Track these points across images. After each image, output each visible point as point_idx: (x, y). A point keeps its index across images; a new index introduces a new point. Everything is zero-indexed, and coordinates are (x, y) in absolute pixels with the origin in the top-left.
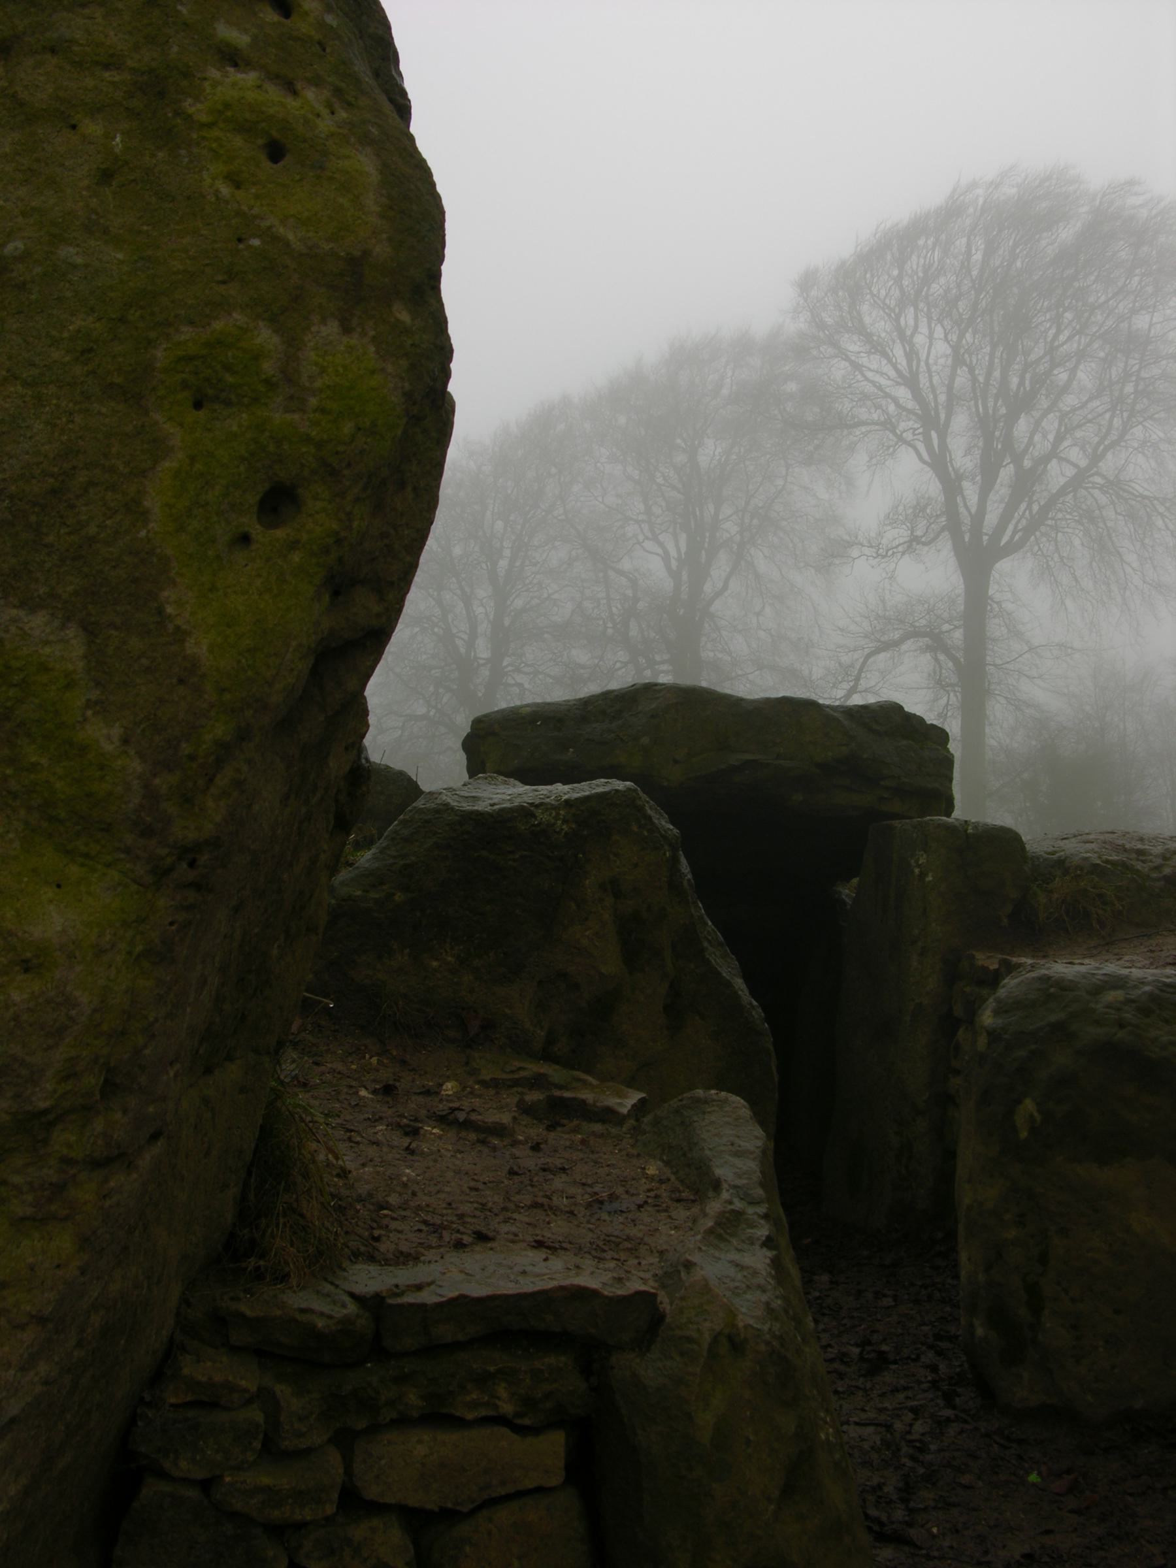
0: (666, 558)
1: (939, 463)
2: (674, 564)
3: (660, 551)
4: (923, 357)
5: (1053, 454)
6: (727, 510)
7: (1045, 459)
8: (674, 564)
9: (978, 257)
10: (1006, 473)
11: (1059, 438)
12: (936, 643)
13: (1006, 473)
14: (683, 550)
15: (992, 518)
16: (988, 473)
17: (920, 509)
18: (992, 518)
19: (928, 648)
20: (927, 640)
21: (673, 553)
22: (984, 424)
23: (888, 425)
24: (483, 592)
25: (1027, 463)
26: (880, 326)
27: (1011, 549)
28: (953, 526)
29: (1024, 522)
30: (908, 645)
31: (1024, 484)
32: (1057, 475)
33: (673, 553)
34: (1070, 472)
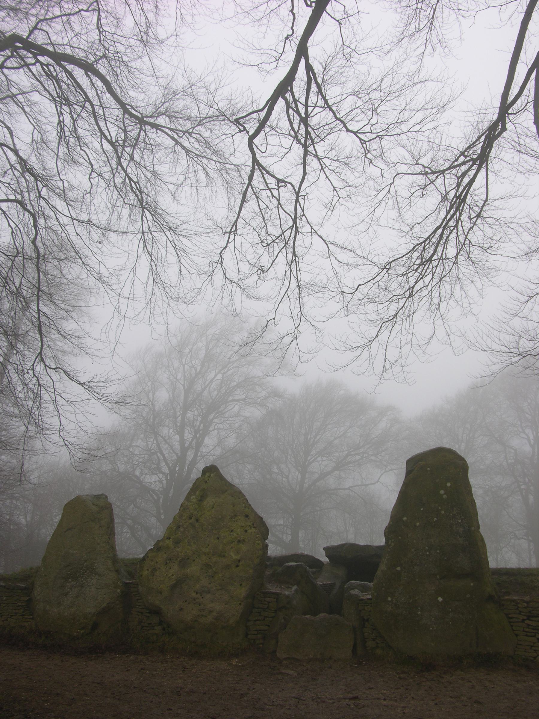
2: (532, 442)
3: (526, 437)
8: (532, 442)
21: (531, 437)
33: (531, 437)
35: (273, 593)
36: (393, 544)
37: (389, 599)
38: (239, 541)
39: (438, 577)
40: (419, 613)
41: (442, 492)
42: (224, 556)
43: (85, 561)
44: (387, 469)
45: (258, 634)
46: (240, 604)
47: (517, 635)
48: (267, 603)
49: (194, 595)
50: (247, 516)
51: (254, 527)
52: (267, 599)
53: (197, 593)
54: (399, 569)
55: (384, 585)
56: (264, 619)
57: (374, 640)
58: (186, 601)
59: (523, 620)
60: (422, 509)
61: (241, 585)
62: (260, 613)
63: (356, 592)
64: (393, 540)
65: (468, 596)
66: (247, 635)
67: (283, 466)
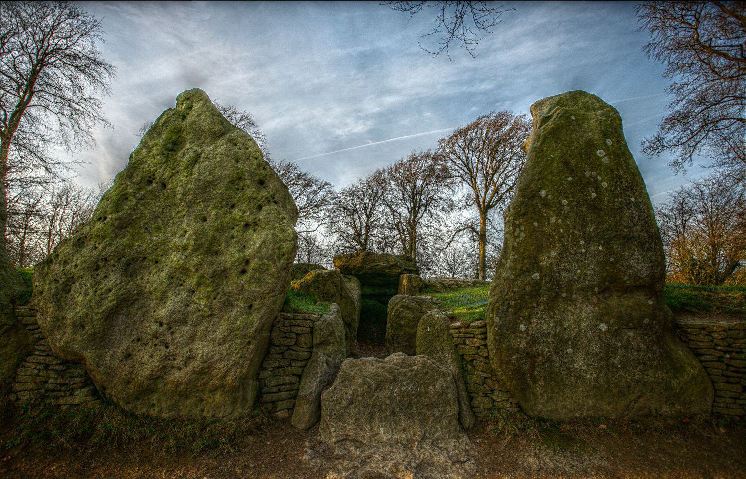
0: (408, 209)
1: (474, 186)
2: (410, 210)
5: (503, 183)
6: (423, 197)
7: (501, 184)
8: (410, 210)
9: (484, 135)
10: (492, 187)
11: (505, 179)
12: (472, 229)
13: (492, 187)
15: (487, 200)
16: (487, 187)
17: (468, 198)
19: (472, 232)
22: (486, 176)
23: (461, 176)
24: (364, 217)
27: (493, 206)
29: (496, 200)
30: (465, 231)
31: (496, 192)
32: (504, 188)
34: (508, 187)
36: (523, 235)
37: (523, 328)
38: (247, 225)
39: (596, 290)
40: (570, 350)
42: (217, 253)
44: (323, 222)
45: (280, 391)
46: (249, 343)
48: (294, 336)
51: (275, 203)
53: (161, 324)
54: (536, 275)
55: (512, 303)
56: (290, 365)
57: (486, 395)
58: (139, 340)
60: (570, 179)
61: (251, 306)
62: (283, 353)
64: (523, 228)
65: (646, 321)
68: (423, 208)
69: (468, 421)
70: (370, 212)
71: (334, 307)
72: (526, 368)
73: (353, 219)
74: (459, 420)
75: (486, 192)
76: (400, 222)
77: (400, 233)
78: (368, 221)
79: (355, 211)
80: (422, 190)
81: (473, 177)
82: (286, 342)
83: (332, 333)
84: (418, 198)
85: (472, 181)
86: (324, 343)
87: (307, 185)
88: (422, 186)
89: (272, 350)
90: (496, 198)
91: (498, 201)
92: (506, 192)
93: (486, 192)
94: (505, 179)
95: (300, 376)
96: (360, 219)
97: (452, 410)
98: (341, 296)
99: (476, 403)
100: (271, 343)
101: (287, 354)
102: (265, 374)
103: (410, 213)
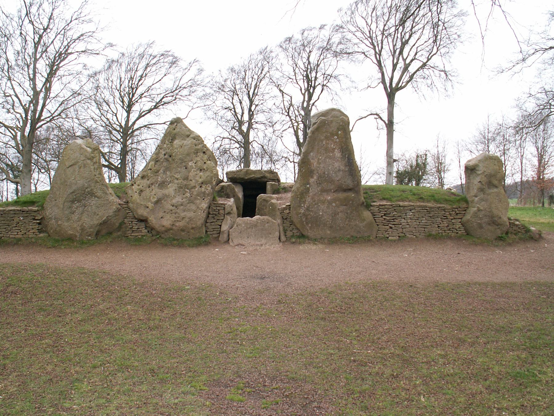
0: (301, 90)
2: (303, 91)
4: (374, 32)
10: (401, 64)
13: (401, 64)
14: (306, 87)
15: (395, 81)
16: (395, 66)
18: (395, 81)
20: (376, 116)
24: (246, 98)
25: (408, 61)
26: (362, 23)
27: (402, 88)
28: (383, 82)
29: (405, 80)
35: (222, 204)
37: (302, 205)
41: (336, 137)
43: (87, 188)
47: (378, 225)
49: (171, 208)
50: (204, 152)
52: (218, 208)
54: (308, 186)
57: (291, 231)
59: (382, 216)
63: (274, 201)
66: (206, 231)
67: (112, 106)
68: (318, 89)
69: (283, 238)
70: (254, 93)
71: (232, 200)
72: (304, 219)
73: (232, 103)
74: (279, 238)
75: (394, 70)
76: (291, 105)
77: (291, 120)
78: (251, 106)
79: (235, 92)
80: (318, 65)
81: (378, 54)
82: (214, 212)
83: (232, 210)
84: (313, 74)
85: (376, 58)
86: (229, 213)
87: (173, 63)
88: (318, 61)
89: (210, 216)
90: (406, 78)
91: (408, 82)
92: (418, 70)
93: (394, 70)
94: (416, 54)
95: (221, 226)
96: (241, 103)
97: (277, 234)
98: (235, 196)
99: (287, 234)
100: (209, 213)
101: (216, 217)
102: (208, 224)
103: (304, 95)
